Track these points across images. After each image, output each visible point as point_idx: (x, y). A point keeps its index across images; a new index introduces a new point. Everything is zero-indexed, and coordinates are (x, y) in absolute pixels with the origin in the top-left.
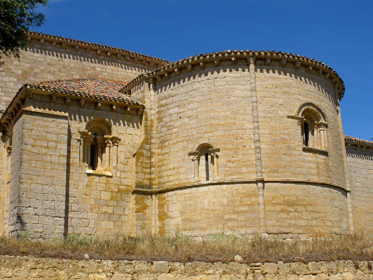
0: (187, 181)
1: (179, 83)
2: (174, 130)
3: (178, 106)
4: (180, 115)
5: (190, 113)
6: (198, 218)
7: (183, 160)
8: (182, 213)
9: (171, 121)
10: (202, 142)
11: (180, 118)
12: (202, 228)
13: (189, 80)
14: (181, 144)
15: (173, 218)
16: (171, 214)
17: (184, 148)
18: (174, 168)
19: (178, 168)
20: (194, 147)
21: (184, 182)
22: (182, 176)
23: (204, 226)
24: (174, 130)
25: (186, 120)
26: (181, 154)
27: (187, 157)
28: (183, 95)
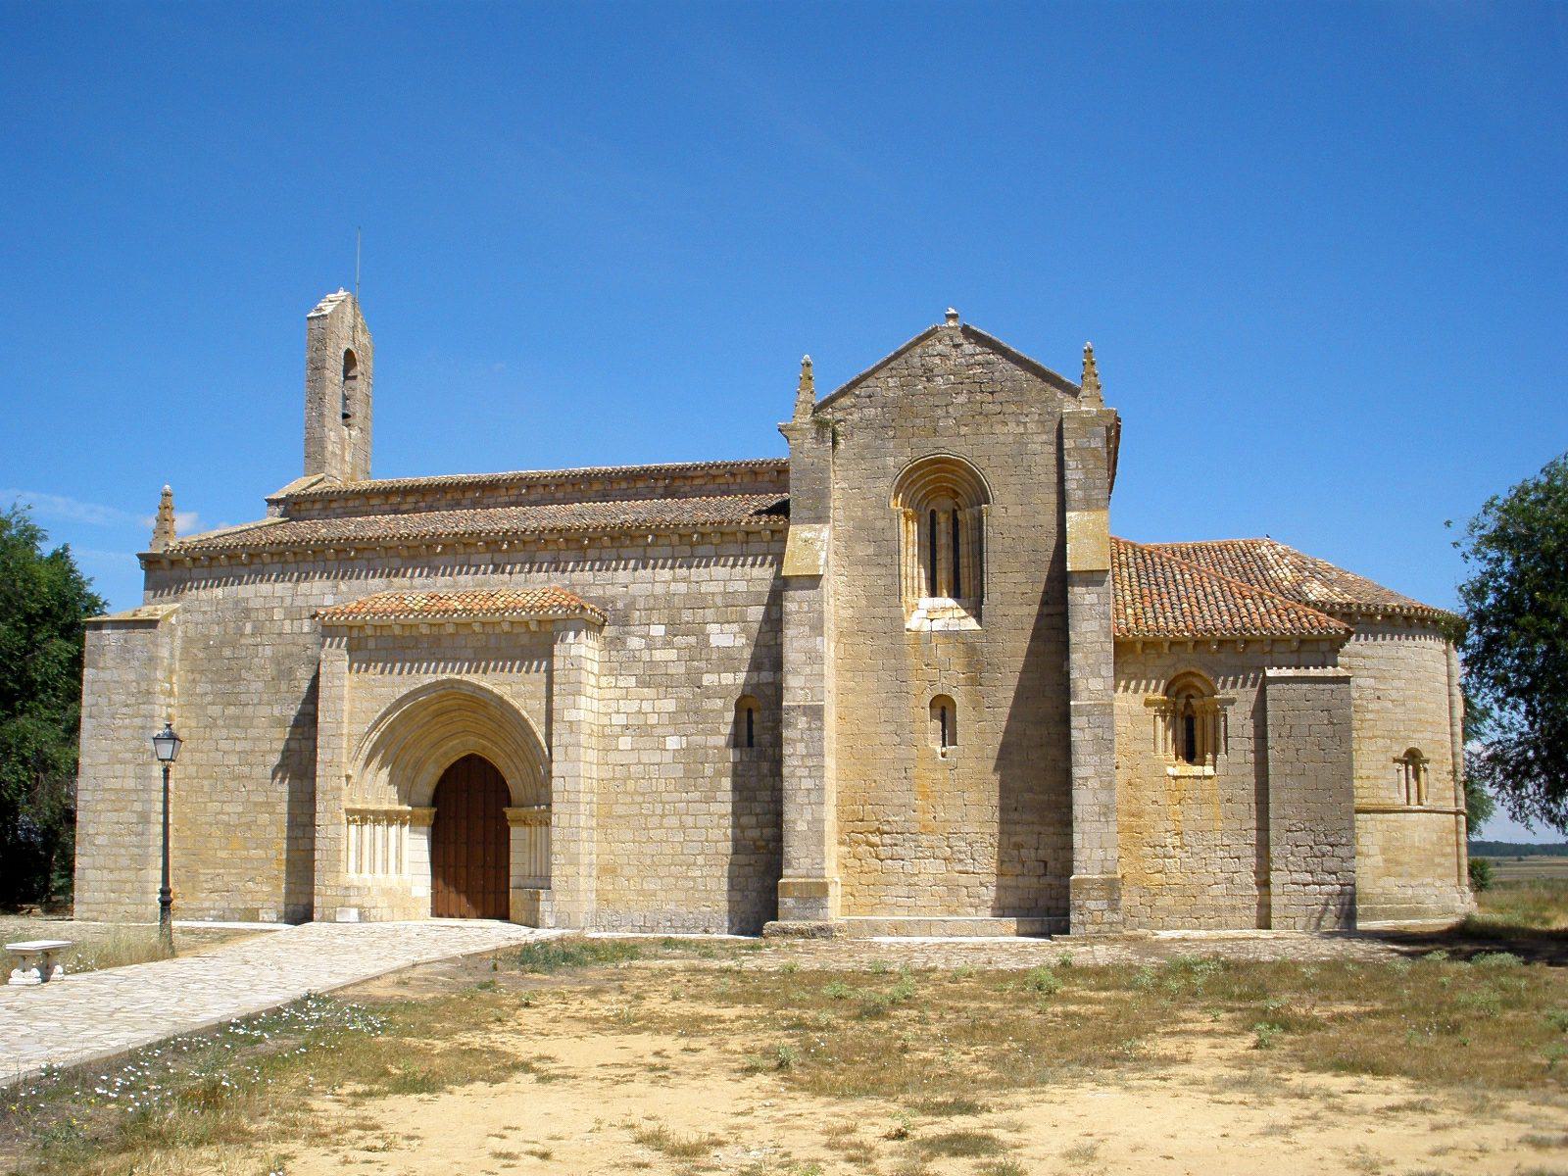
0: (1390, 801)
1: (1375, 640)
2: (1369, 716)
3: (1375, 678)
4: (1377, 693)
5: (1394, 695)
6: (1407, 859)
7: (1384, 767)
8: (1384, 850)
9: (1360, 698)
10: (1412, 745)
11: (1379, 698)
12: (1412, 875)
13: (1392, 639)
14: (1380, 742)
15: (1368, 856)
16: (1364, 849)
17: (1388, 749)
18: (1368, 777)
19: (1376, 778)
20: (1400, 751)
21: (1388, 803)
22: (1382, 793)
23: (1415, 872)
24: (1369, 716)
25: (1390, 705)
26: (1382, 757)
27: (1390, 764)
28: (1382, 661)
